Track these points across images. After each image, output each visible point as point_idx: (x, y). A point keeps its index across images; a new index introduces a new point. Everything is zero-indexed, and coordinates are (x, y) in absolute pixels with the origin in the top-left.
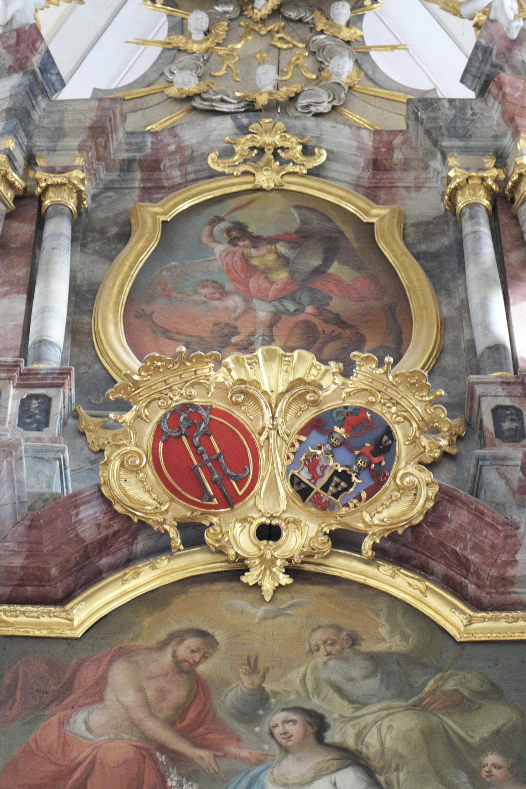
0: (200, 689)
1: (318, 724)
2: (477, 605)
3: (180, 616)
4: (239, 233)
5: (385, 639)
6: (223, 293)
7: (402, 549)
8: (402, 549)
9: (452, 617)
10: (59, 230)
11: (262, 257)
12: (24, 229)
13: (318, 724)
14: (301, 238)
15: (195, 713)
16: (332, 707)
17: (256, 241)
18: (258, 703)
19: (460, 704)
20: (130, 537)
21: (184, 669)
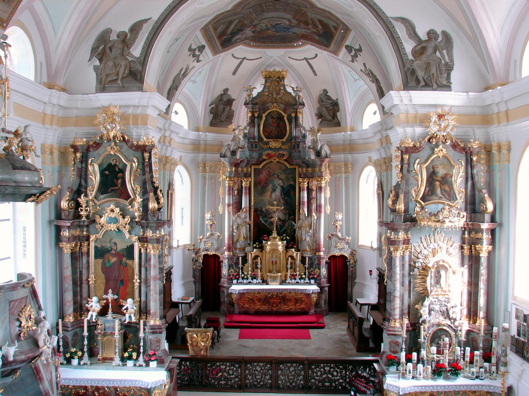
0: (270, 173)
1: (278, 176)
2: (290, 165)
3: (268, 166)
4: (272, 117)
5: (283, 168)
6: (271, 126)
7: (285, 160)
8: (285, 160)
9: (289, 167)
10: (256, 120)
11: (274, 121)
12: (253, 118)
13: (278, 176)
14: (278, 118)
15: (269, 175)
16: (279, 174)
17: (274, 118)
18: (274, 174)
19: (288, 174)
20: (265, 160)
21: (269, 171)
